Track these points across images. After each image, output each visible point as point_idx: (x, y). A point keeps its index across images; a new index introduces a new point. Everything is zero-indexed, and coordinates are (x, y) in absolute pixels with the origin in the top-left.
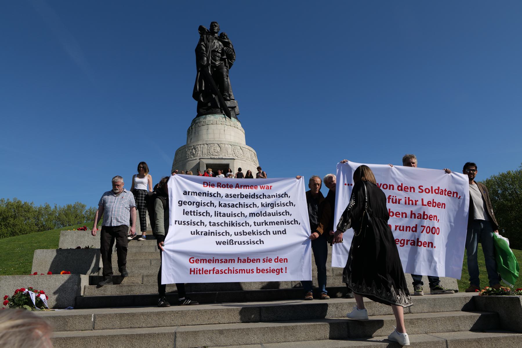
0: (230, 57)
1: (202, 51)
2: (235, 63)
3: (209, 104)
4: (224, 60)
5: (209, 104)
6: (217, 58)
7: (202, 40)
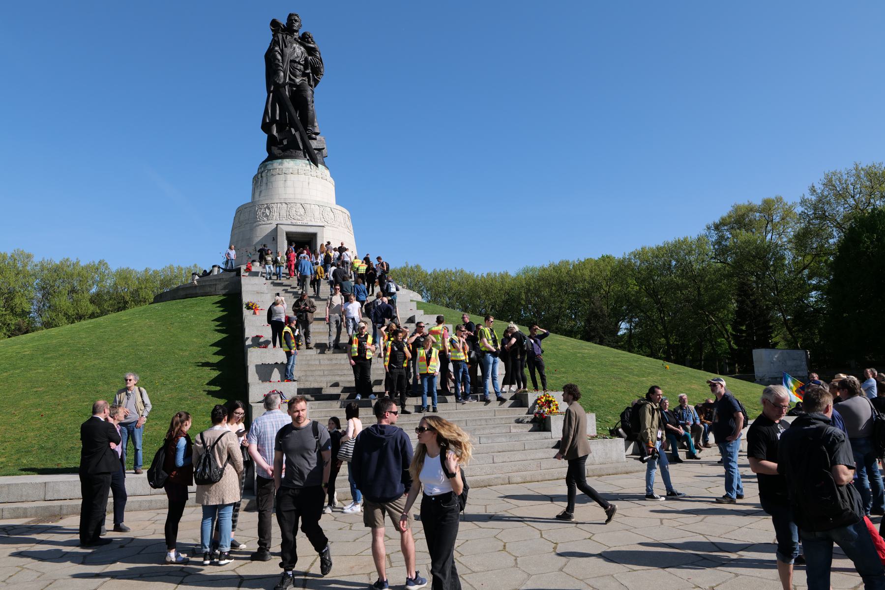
0: (317, 71)
2: (323, 80)
3: (285, 142)
4: (307, 75)
5: (285, 142)
6: (298, 73)
7: (275, 42)
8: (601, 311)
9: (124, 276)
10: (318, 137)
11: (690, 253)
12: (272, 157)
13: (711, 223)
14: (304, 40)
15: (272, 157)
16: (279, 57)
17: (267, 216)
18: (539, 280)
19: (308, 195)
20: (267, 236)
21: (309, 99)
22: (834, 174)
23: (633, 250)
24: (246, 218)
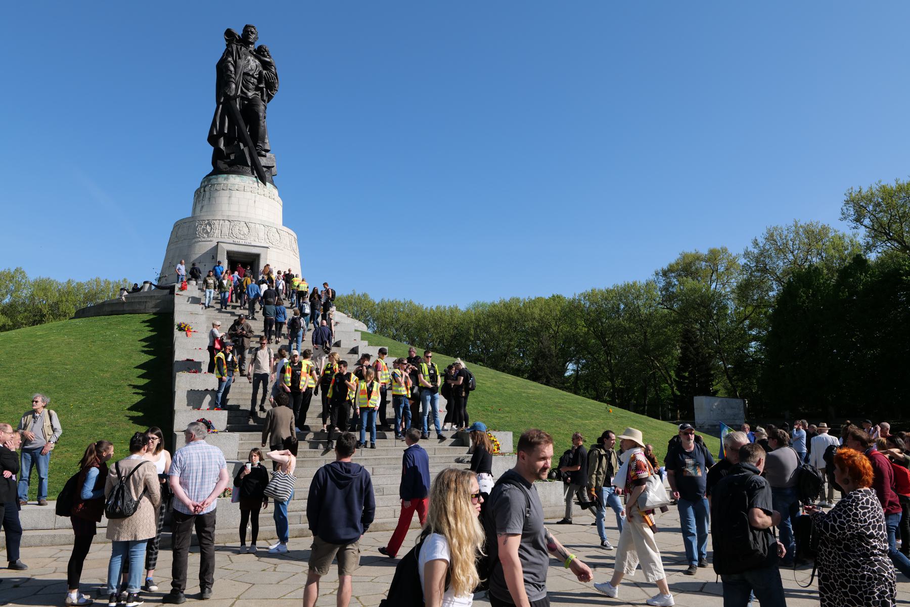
1: (229, 73)
2: (277, 96)
3: (232, 157)
4: (261, 89)
5: (232, 157)
6: (251, 86)
7: (228, 53)
8: (549, 351)
9: (43, 286)
10: (268, 154)
11: (638, 297)
12: (217, 171)
13: (659, 269)
14: (260, 53)
15: (217, 171)
16: (232, 69)
17: (207, 233)
18: (489, 316)
19: (254, 215)
20: (206, 253)
21: (261, 114)
22: (776, 229)
23: (583, 291)
24: (184, 234)
